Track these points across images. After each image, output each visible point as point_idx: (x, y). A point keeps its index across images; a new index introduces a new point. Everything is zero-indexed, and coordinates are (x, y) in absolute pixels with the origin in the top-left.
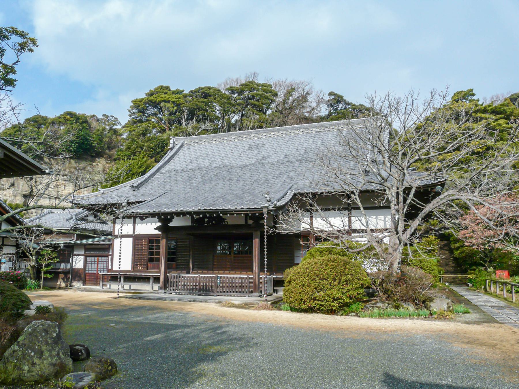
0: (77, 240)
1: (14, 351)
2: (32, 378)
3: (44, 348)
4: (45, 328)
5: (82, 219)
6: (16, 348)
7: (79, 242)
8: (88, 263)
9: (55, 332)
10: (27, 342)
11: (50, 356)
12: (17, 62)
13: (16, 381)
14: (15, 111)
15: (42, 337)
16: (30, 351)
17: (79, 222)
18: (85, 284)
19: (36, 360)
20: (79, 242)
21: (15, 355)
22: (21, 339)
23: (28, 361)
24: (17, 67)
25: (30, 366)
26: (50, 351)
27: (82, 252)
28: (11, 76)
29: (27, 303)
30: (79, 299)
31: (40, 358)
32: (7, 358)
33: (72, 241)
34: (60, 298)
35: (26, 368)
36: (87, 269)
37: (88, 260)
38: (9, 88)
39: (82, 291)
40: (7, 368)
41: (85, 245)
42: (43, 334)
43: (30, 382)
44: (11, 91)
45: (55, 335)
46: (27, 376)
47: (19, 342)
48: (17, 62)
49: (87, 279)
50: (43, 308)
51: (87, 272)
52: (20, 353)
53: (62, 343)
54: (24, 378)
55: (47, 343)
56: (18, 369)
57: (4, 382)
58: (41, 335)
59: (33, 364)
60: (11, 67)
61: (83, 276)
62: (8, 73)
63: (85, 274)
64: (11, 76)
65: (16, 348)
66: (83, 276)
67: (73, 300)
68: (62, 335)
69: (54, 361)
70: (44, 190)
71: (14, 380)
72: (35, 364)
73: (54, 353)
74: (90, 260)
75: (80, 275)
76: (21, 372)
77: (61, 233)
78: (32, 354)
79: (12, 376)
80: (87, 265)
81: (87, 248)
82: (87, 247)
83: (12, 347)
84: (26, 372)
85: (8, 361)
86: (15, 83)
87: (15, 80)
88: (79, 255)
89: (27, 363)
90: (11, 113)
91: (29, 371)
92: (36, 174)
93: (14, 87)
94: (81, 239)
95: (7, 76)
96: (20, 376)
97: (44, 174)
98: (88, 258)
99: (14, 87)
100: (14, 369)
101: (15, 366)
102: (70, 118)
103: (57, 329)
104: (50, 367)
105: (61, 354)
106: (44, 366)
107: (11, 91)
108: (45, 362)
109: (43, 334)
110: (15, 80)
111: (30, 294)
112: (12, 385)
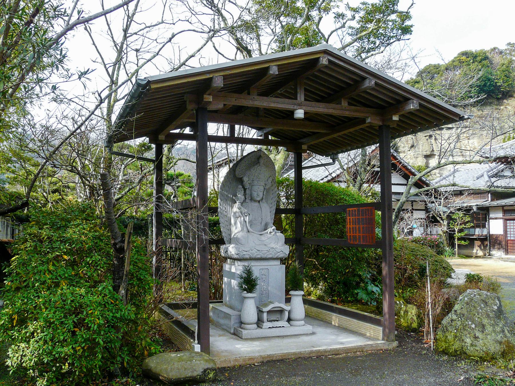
0: (492, 201)
1: (452, 320)
2: (476, 354)
3: (485, 321)
4: (482, 298)
5: (496, 175)
6: (454, 317)
7: (495, 203)
8: (508, 227)
9: (495, 305)
10: (464, 311)
11: (494, 331)
12: (412, 5)
13: (458, 353)
14: (417, 60)
15: (481, 308)
16: (470, 323)
17: (493, 180)
18: (507, 252)
19: (478, 334)
20: (495, 203)
21: (453, 324)
22: (457, 307)
23: (469, 334)
24: (412, 12)
25: (472, 339)
26: (493, 325)
27: (501, 215)
28: (407, 23)
29: (448, 271)
30: (504, 271)
31: (483, 332)
32: (446, 327)
33: (487, 201)
34: (480, 268)
35: (468, 341)
36: (509, 235)
37: (508, 224)
38: (407, 36)
39: (505, 261)
40: (447, 337)
41: (503, 207)
42: (482, 305)
43: (474, 357)
44: (408, 39)
45: (496, 308)
46: (470, 350)
47: (456, 311)
48: (412, 5)
49: (509, 248)
50: (473, 276)
51: (509, 238)
52: (459, 323)
53: (505, 318)
54: (467, 352)
55: (488, 316)
56: (459, 340)
57: (446, 351)
58: (480, 306)
59: (476, 338)
60: (407, 13)
61: (504, 243)
62: (403, 21)
63: (507, 241)
64: (407, 23)
65: (454, 317)
66: (504, 243)
67: (497, 270)
68: (503, 309)
69: (499, 338)
70: (454, 144)
71: (456, 351)
72: (478, 337)
73: (498, 329)
74: (512, 224)
75: (501, 242)
76: (463, 344)
77: (477, 193)
78: (473, 326)
79: (454, 347)
80: (508, 230)
81: (506, 210)
82: (505, 208)
83: (450, 315)
84: (469, 345)
85: (447, 330)
86: (412, 29)
87: (412, 26)
88: (496, 219)
89: (468, 335)
90: (412, 62)
91: (472, 345)
92: (453, 121)
93: (411, 34)
94: (498, 199)
95: (403, 24)
96: (462, 348)
97: (463, 121)
98: (508, 222)
99: (411, 34)
100: (455, 339)
101: (456, 337)
102: (469, 58)
103: (498, 302)
104: (496, 345)
105: (506, 332)
106: (489, 342)
107: (408, 39)
108: (489, 337)
109: (482, 305)
110: (412, 26)
111: (454, 261)
112: (455, 356)
